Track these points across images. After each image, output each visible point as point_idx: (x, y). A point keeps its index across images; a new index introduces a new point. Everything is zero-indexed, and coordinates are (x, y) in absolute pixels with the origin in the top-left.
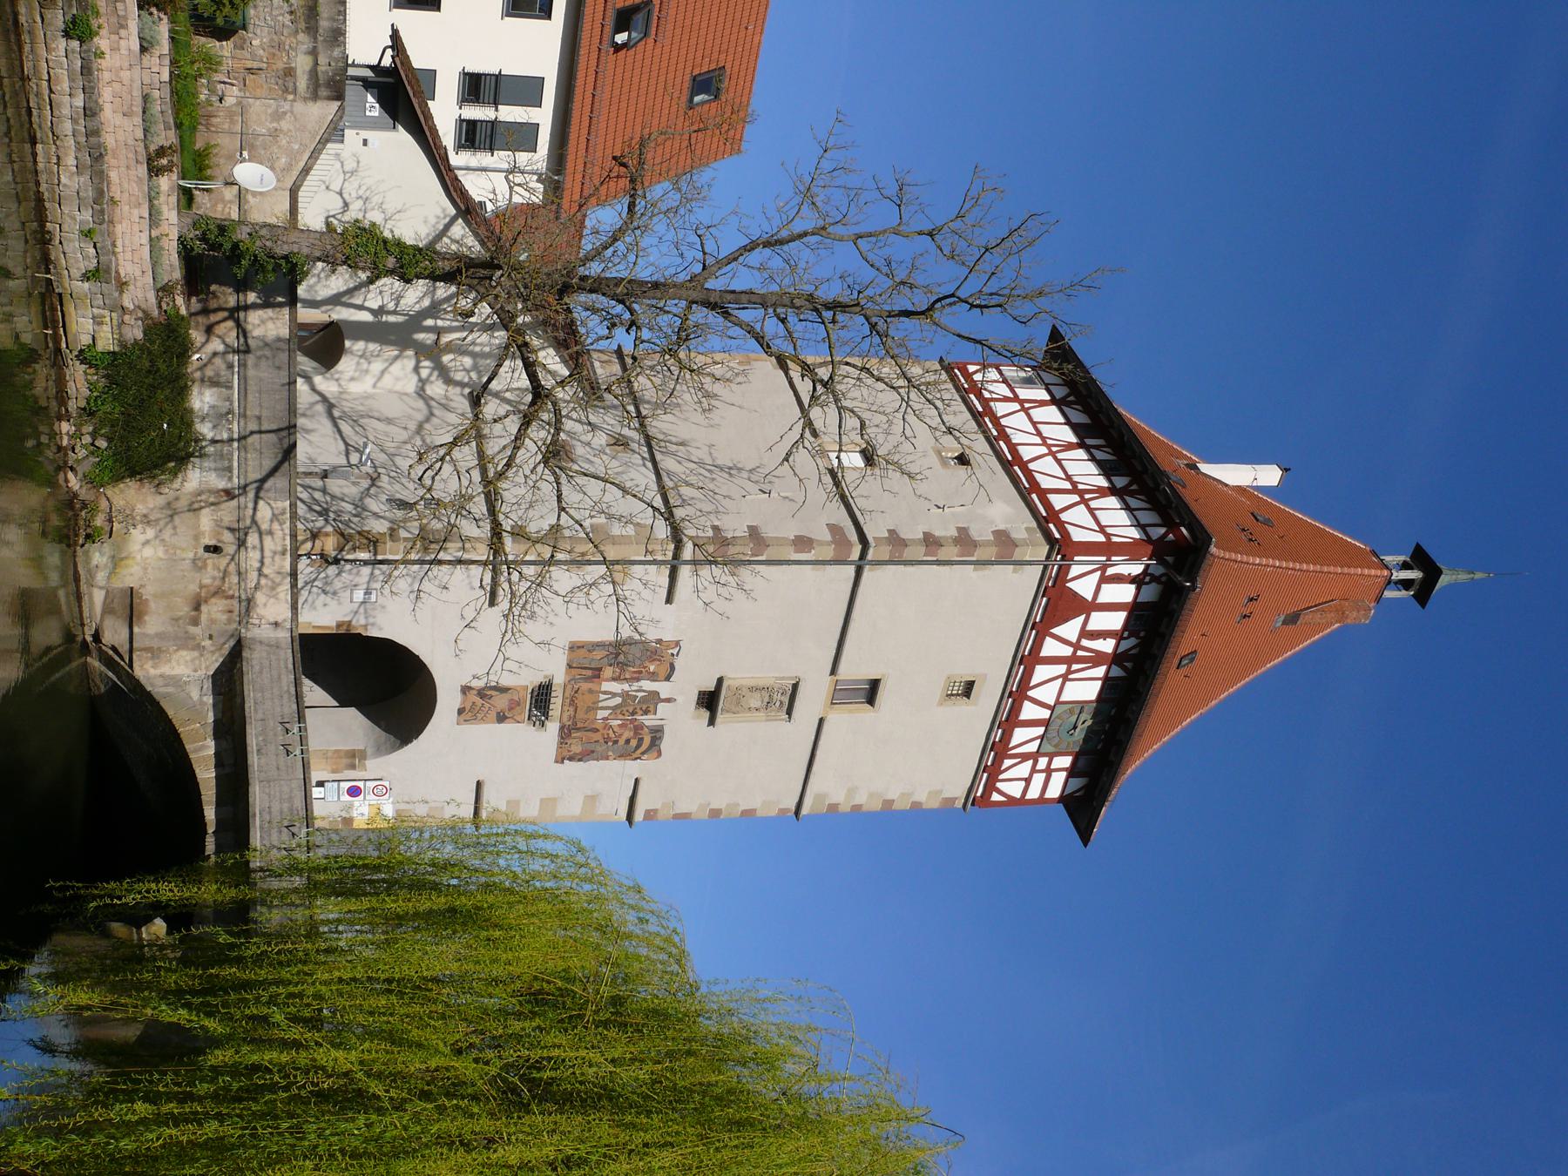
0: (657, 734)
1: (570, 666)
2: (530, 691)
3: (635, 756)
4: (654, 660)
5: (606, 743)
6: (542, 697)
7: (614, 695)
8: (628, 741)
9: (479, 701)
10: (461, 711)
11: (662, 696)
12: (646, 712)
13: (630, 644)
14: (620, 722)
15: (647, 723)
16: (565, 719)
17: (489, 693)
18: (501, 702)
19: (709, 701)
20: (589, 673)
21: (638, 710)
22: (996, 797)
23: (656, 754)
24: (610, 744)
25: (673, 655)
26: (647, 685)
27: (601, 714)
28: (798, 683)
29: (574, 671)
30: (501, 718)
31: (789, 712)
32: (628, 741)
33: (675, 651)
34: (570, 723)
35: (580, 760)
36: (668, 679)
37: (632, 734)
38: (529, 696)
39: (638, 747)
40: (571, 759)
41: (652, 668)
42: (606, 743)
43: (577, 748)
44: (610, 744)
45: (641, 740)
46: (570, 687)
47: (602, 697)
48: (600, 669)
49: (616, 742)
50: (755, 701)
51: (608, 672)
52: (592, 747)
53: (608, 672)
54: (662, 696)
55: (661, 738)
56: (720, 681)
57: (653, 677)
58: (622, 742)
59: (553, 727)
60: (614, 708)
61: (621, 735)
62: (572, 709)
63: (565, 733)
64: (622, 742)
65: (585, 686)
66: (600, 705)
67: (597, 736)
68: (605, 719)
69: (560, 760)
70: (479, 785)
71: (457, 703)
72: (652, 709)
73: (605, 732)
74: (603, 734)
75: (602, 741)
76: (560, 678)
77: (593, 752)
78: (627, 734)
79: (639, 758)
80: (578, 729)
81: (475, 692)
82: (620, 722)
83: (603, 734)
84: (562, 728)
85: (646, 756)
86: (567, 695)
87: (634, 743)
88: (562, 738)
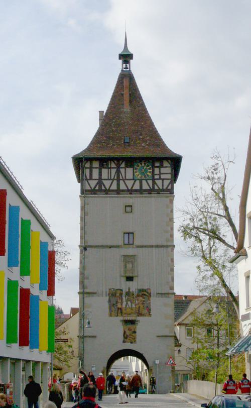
1: (117, 316)
6: (126, 322)
7: (127, 303)
8: (144, 298)
9: (129, 338)
10: (131, 343)
11: (128, 291)
12: (133, 294)
13: (110, 301)
15: (137, 293)
16: (135, 315)
18: (128, 333)
19: (130, 279)
22: (169, 187)
23: (149, 290)
27: (134, 306)
28: (124, 256)
29: (119, 314)
30: (135, 332)
31: (135, 256)
40: (150, 313)
43: (145, 311)
47: (128, 306)
48: (118, 308)
49: (144, 301)
50: (129, 266)
53: (119, 306)
54: (128, 291)
55: (143, 289)
57: (121, 294)
58: (144, 300)
59: (139, 318)
60: (131, 303)
63: (140, 314)
64: (144, 300)
65: (124, 311)
66: (130, 306)
67: (141, 306)
69: (150, 315)
71: (129, 343)
76: (121, 318)
77: (147, 307)
80: (139, 312)
81: (125, 340)
84: (138, 316)
85: (149, 292)
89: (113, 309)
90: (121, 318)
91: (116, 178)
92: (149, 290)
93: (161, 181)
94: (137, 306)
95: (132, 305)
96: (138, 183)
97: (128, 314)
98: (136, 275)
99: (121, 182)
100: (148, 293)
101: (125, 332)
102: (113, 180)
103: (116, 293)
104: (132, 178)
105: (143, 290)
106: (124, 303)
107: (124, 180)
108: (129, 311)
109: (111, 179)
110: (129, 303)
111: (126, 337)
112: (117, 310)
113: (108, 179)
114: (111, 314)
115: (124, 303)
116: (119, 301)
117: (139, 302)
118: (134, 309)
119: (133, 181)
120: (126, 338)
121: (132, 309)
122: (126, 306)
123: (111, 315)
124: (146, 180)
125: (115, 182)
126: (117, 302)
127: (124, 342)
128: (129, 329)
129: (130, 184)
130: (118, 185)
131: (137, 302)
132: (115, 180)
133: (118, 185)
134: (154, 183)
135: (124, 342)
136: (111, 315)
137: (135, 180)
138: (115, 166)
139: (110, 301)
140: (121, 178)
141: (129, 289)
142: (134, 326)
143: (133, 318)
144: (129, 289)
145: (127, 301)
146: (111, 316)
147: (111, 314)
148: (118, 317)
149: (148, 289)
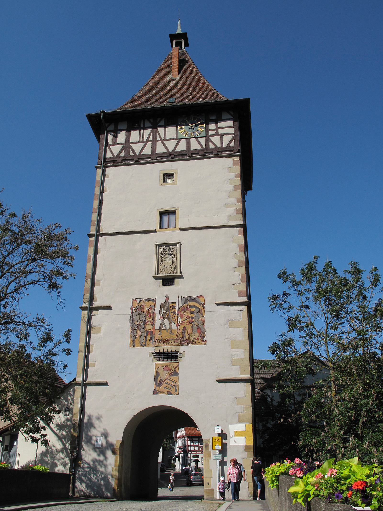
0: (186, 300)
2: (159, 362)
3: (202, 308)
4: (143, 309)
5: (193, 322)
8: (192, 312)
9: (164, 385)
10: (169, 393)
12: (174, 307)
13: (133, 320)
14: (179, 319)
16: (177, 344)
17: (158, 381)
18: (163, 375)
20: (149, 336)
21: (172, 311)
23: (201, 299)
24: (193, 320)
25: (140, 301)
26: (157, 311)
27: (174, 326)
29: (148, 342)
30: (176, 373)
31: (175, 244)
32: (192, 312)
33: (138, 300)
34: (179, 341)
35: (204, 333)
36: (154, 301)
37: (187, 311)
38: (162, 362)
39: (195, 307)
40: (203, 337)
41: (147, 308)
42: (193, 322)
44: (193, 320)
45: (191, 306)
46: (157, 344)
47: (163, 328)
48: (147, 332)
49: (192, 318)
51: (149, 327)
52: (195, 329)
53: (149, 327)
55: (190, 298)
56: (156, 278)
57: (152, 308)
58: (192, 315)
59: (182, 349)
61: (188, 316)
62: (171, 341)
63: (185, 342)
64: (192, 315)
65: (157, 337)
66: (168, 328)
67: (188, 327)
68: (177, 325)
69: (204, 342)
70: (219, 381)
71: (166, 396)
72: (172, 305)
73: (185, 324)
74: (187, 325)
75: (191, 325)
76: (151, 349)
78: (187, 313)
79: (203, 306)
80: (183, 337)
81: (158, 388)
82: (179, 319)
83: (187, 325)
84: (183, 344)
86: (162, 344)
87: (193, 309)
88: (189, 343)
89: (138, 333)
90: (151, 349)
91: (150, 139)
92: (201, 301)
93: (219, 137)
94: (181, 327)
95: (170, 325)
96: (183, 142)
97: (164, 341)
98: (178, 273)
99: (159, 144)
100: (200, 304)
101: (157, 374)
102: (148, 141)
103: (142, 306)
104: (175, 137)
105: (191, 299)
106: (158, 323)
107: (162, 141)
108: (165, 336)
109: (143, 142)
110: (166, 322)
111: (158, 382)
112: (144, 334)
113: (139, 142)
114: (134, 342)
115: (158, 323)
116: (150, 319)
117: (184, 319)
118: (175, 332)
119: (176, 141)
120: (160, 384)
121: (170, 331)
122: (161, 326)
123: (133, 344)
124: (196, 138)
125: (149, 145)
126: (145, 322)
127: (156, 392)
128: (166, 368)
129: (171, 145)
130: (154, 148)
131: (180, 319)
132: (150, 141)
133: (154, 148)
134: (208, 141)
135: (156, 392)
136: (133, 344)
137: (180, 140)
138: (151, 125)
139: (133, 320)
140: (158, 138)
141: (167, 298)
142: (173, 363)
143: (173, 349)
144: (167, 298)
145: (162, 318)
146: (134, 346)
147: (134, 342)
148: (145, 348)
149: (199, 297)
